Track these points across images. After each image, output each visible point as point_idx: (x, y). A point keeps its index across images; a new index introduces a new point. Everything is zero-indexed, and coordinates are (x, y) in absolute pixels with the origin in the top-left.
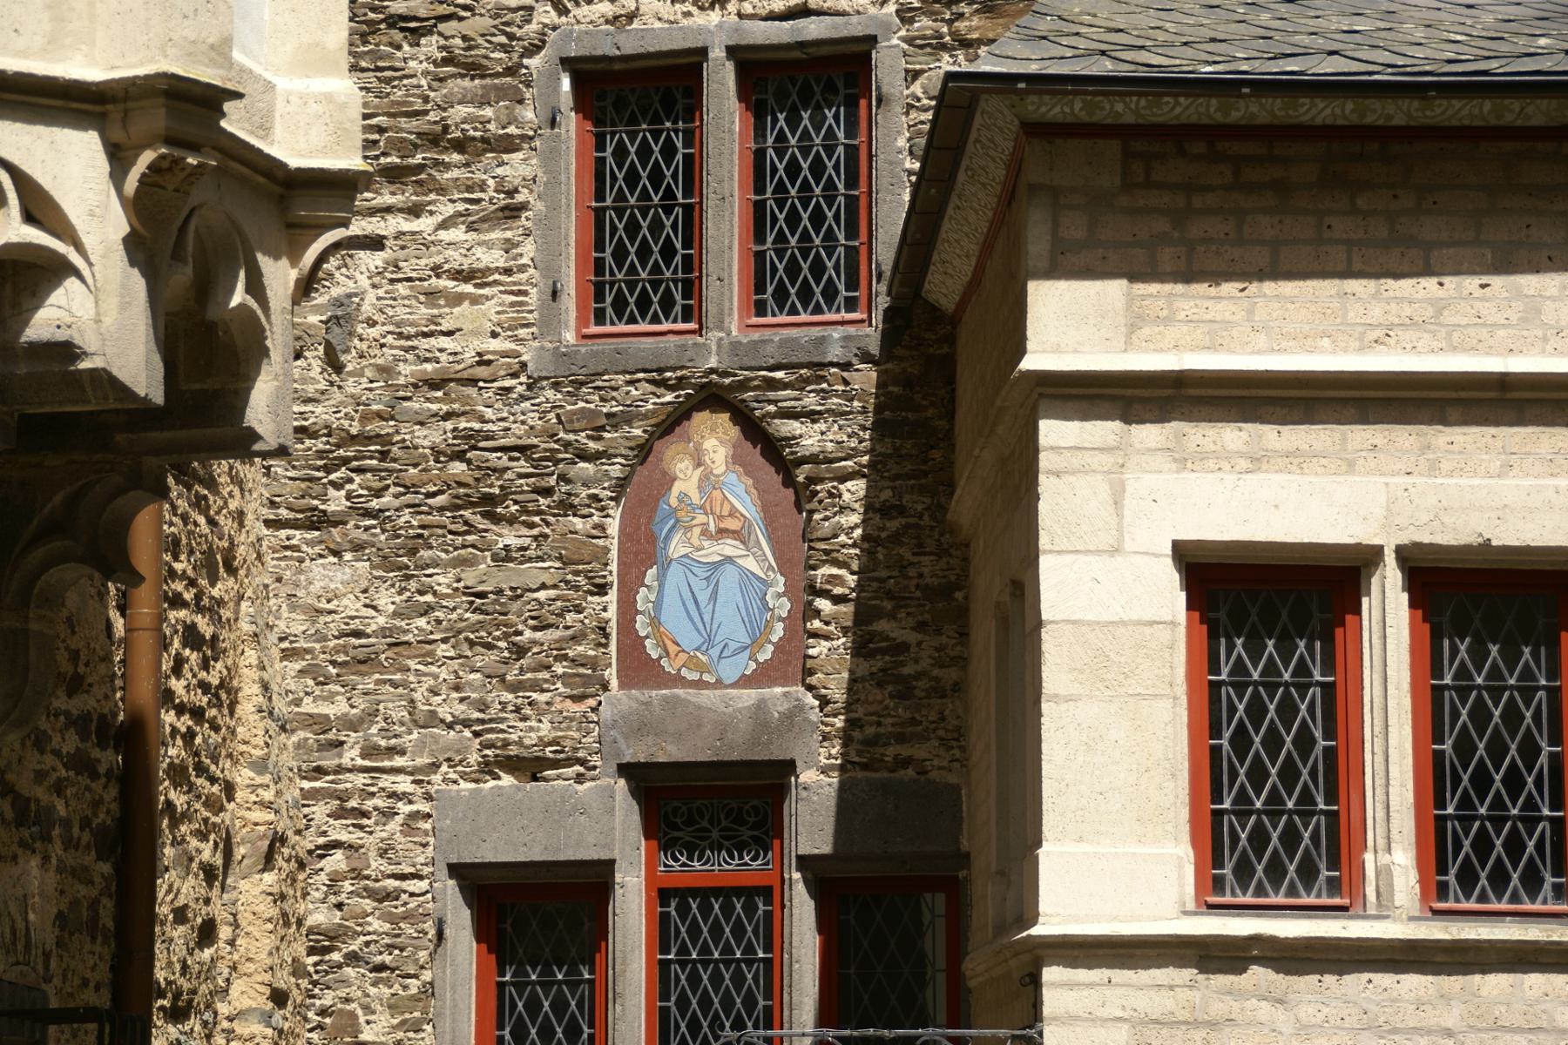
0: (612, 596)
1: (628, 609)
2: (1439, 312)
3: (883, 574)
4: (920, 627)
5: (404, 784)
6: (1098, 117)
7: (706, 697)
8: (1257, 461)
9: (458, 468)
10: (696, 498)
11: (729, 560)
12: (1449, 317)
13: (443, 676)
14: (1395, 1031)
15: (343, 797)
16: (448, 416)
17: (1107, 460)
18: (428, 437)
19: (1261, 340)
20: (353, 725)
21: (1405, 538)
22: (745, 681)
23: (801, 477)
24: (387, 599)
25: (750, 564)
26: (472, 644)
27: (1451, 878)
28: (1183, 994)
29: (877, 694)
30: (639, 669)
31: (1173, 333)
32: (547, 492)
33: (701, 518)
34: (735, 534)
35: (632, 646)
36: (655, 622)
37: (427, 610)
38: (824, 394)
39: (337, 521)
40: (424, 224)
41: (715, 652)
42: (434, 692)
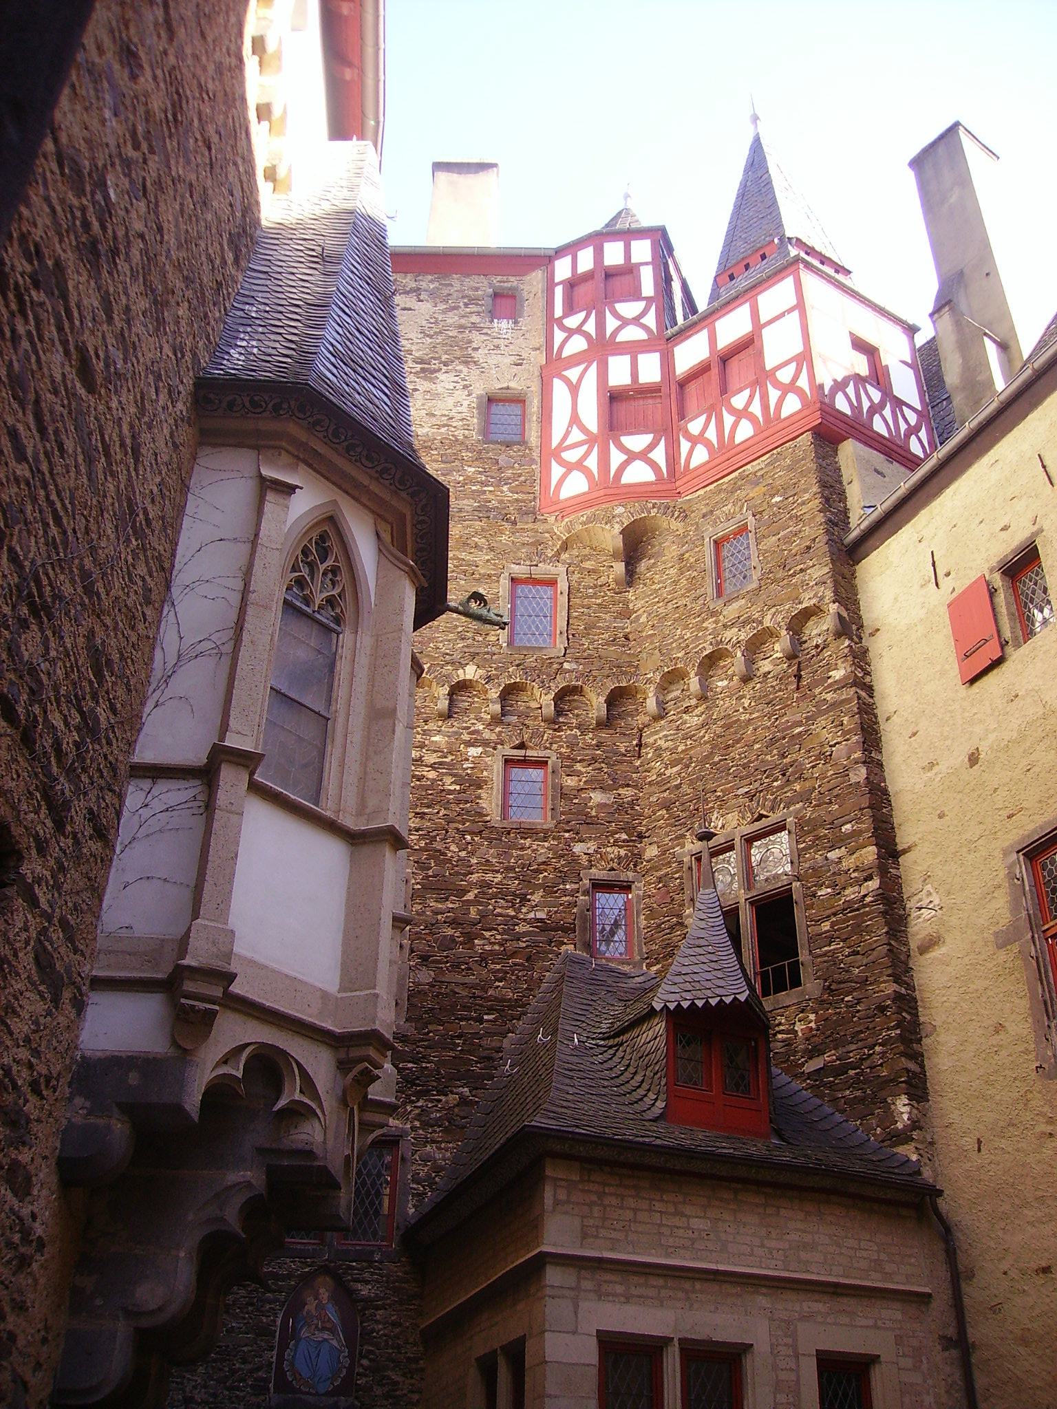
0: (275, 1352)
1: (281, 1357)
2: (693, 1244)
3: (390, 1351)
4: (404, 1375)
7: (310, 1398)
8: (628, 1299)
10: (314, 1312)
11: (326, 1340)
12: (696, 1246)
13: (199, 1381)
17: (572, 1293)
19: (630, 1248)
22: (328, 1394)
23: (360, 1306)
25: (335, 1343)
26: (213, 1368)
29: (385, 1403)
30: (283, 1385)
32: (252, 1304)
33: (315, 1322)
34: (328, 1329)
35: (280, 1373)
36: (292, 1364)
38: (372, 1274)
41: (316, 1379)
42: (195, 1387)
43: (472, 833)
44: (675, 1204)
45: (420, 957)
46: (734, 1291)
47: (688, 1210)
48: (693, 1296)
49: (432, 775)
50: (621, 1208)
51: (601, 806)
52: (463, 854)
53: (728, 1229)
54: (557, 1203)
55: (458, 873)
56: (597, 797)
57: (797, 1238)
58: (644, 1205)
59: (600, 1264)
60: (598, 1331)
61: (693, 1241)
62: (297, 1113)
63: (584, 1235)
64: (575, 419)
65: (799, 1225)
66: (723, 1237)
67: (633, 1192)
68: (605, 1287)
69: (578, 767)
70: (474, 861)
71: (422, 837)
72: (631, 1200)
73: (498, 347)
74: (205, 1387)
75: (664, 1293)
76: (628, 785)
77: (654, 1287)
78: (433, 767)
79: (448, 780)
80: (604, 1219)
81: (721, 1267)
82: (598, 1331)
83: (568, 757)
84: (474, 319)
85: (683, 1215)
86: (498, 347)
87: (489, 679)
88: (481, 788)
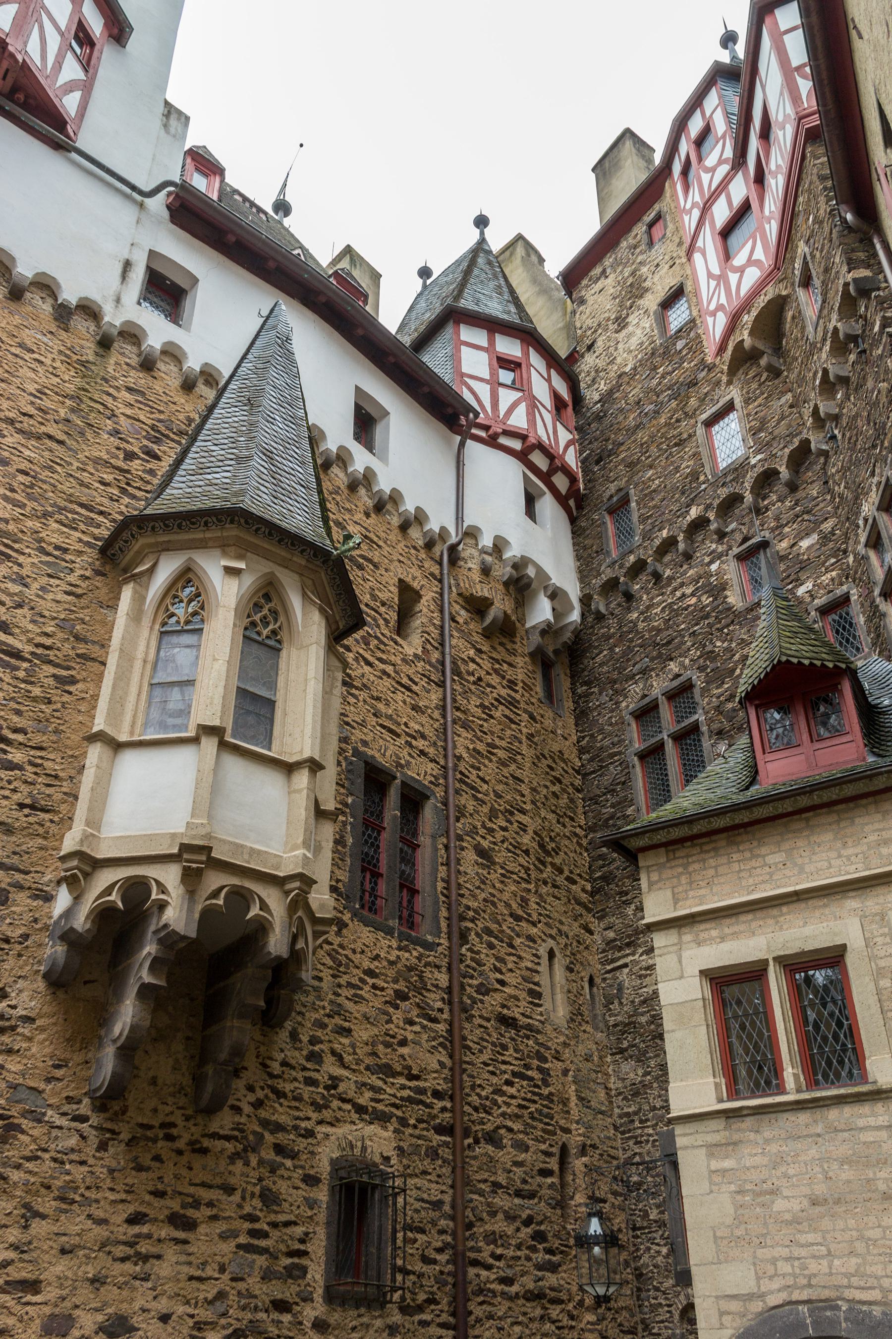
5: (651, 1131)
6: (655, 841)
8: (723, 939)
9: (653, 1027)
12: (775, 877)
14: (799, 1137)
15: (636, 1137)
16: (648, 1011)
17: (675, 948)
18: (643, 1019)
19: (716, 898)
20: (636, 1113)
21: (775, 955)
24: (640, 1072)
27: (820, 1077)
28: (722, 1133)
31: (688, 903)
37: (649, 1073)
39: (626, 1050)
40: (637, 957)
43: (728, 626)
44: (751, 850)
45: (717, 734)
46: (821, 903)
47: (764, 850)
48: (782, 919)
49: (694, 600)
50: (705, 869)
51: (809, 548)
52: (725, 644)
53: (804, 854)
54: (651, 884)
55: (726, 660)
56: (805, 544)
57: (876, 838)
58: (723, 860)
59: (692, 920)
60: (701, 972)
61: (771, 875)
62: (162, 906)
63: (676, 901)
64: (710, 275)
65: (877, 826)
66: (799, 861)
67: (712, 854)
68: (702, 935)
69: (787, 529)
70: (733, 645)
71: (697, 649)
72: (711, 861)
73: (658, 265)
74: (660, 1096)
75: (754, 924)
76: (826, 519)
77: (744, 922)
78: (693, 595)
79: (704, 598)
80: (691, 883)
81: (798, 888)
82: (701, 972)
83: (777, 527)
84: (640, 258)
85: (758, 856)
86: (658, 265)
87: (708, 507)
88: (725, 589)
